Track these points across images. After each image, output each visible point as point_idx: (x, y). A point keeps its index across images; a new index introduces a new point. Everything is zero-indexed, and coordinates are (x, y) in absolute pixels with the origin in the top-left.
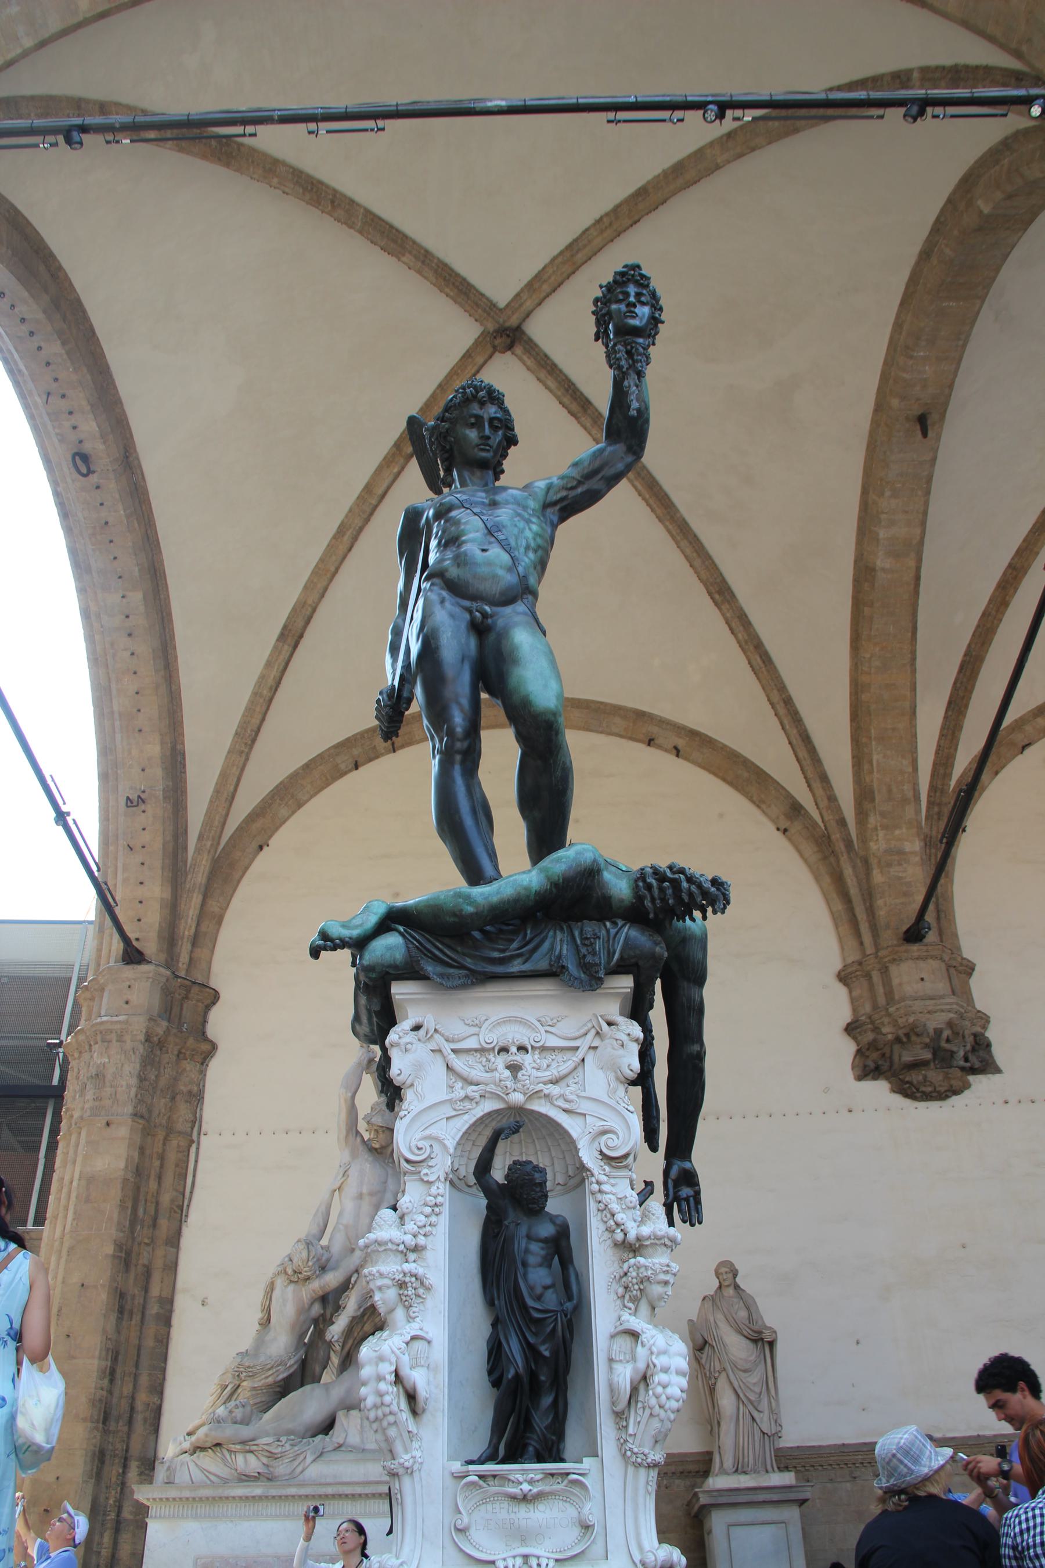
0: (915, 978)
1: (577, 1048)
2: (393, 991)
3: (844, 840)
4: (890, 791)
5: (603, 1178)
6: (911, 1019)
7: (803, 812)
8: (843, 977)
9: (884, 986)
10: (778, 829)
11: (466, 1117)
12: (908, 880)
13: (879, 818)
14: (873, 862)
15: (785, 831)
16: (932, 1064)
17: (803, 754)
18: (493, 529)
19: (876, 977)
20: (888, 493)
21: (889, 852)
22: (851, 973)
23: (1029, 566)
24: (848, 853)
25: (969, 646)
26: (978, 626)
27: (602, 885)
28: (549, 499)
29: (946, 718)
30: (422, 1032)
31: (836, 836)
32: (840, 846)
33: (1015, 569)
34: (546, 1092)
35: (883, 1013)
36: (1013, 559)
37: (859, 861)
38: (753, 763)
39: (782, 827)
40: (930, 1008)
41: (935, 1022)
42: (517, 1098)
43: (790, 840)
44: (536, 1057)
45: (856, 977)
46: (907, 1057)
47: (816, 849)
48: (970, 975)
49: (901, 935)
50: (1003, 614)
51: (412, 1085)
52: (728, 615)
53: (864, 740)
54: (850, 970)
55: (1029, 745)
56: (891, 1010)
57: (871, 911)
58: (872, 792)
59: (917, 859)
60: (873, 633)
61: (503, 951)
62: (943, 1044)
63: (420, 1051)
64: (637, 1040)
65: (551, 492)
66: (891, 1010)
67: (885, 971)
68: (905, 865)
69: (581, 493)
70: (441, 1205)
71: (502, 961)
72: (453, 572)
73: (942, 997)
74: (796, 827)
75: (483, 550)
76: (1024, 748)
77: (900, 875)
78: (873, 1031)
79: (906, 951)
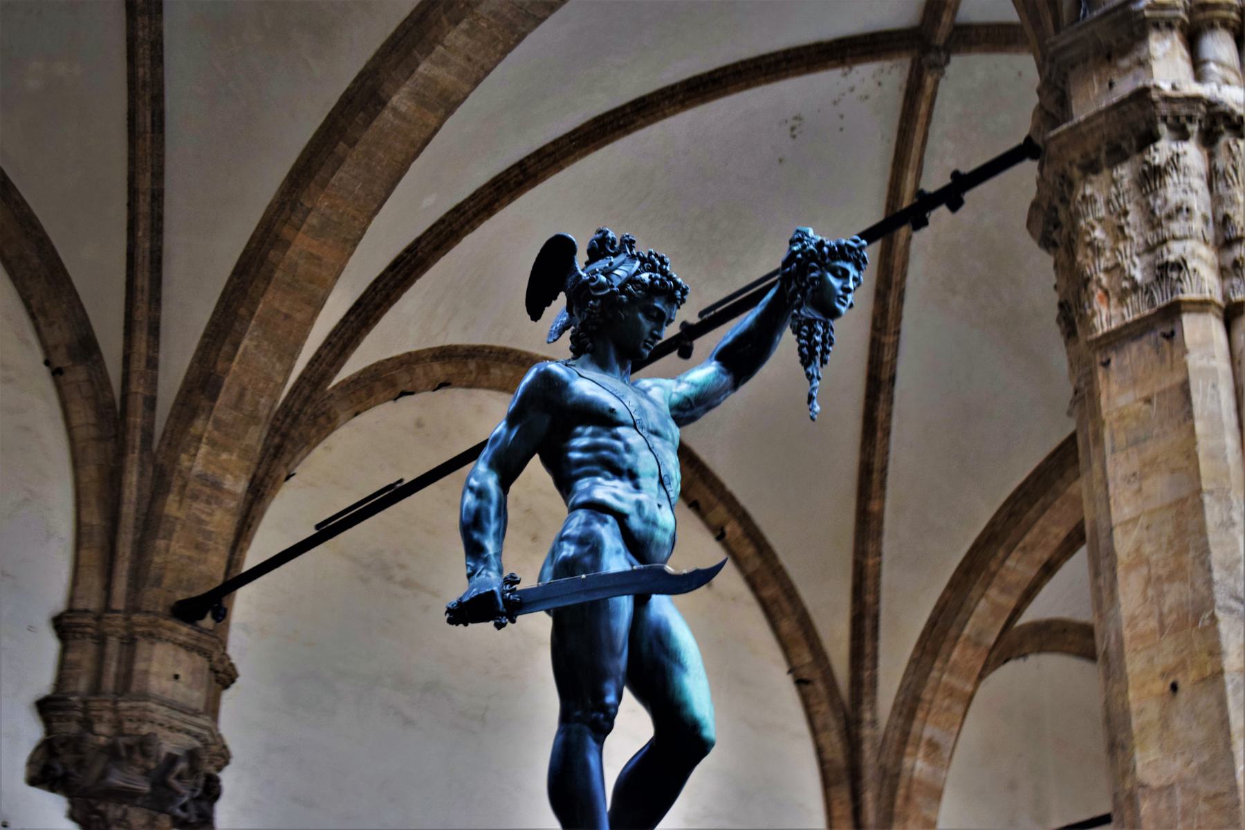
0: (166, 669)
3: (143, 429)
4: (241, 395)
6: (145, 729)
7: (95, 357)
8: (63, 626)
9: (119, 662)
10: (47, 363)
12: (210, 528)
13: (210, 426)
14: (176, 483)
15: (57, 373)
16: (139, 802)
17: (143, 281)
18: (666, 479)
19: (113, 646)
20: (464, 25)
21: (202, 477)
22: (79, 625)
23: (544, 178)
24: (141, 452)
25: (418, 241)
26: (441, 221)
29: (344, 321)
31: (136, 420)
32: (136, 438)
33: (524, 172)
35: (108, 704)
36: (528, 157)
37: (150, 469)
38: (53, 250)
39: (58, 365)
40: (176, 723)
41: (171, 743)
43: (59, 387)
45: (84, 634)
46: (117, 779)
47: (92, 420)
48: (226, 687)
49: (172, 603)
50: (481, 221)
52: (140, 33)
53: (242, 311)
54: (77, 620)
55: (412, 393)
56: (122, 705)
57: (142, 549)
58: (217, 386)
59: (233, 504)
60: (332, 181)
62: (172, 780)
66: (122, 705)
67: (130, 642)
68: (214, 506)
72: (635, 523)
73: (196, 713)
74: (79, 374)
75: (659, 506)
76: (403, 394)
77: (203, 516)
78: (79, 721)
79: (171, 630)
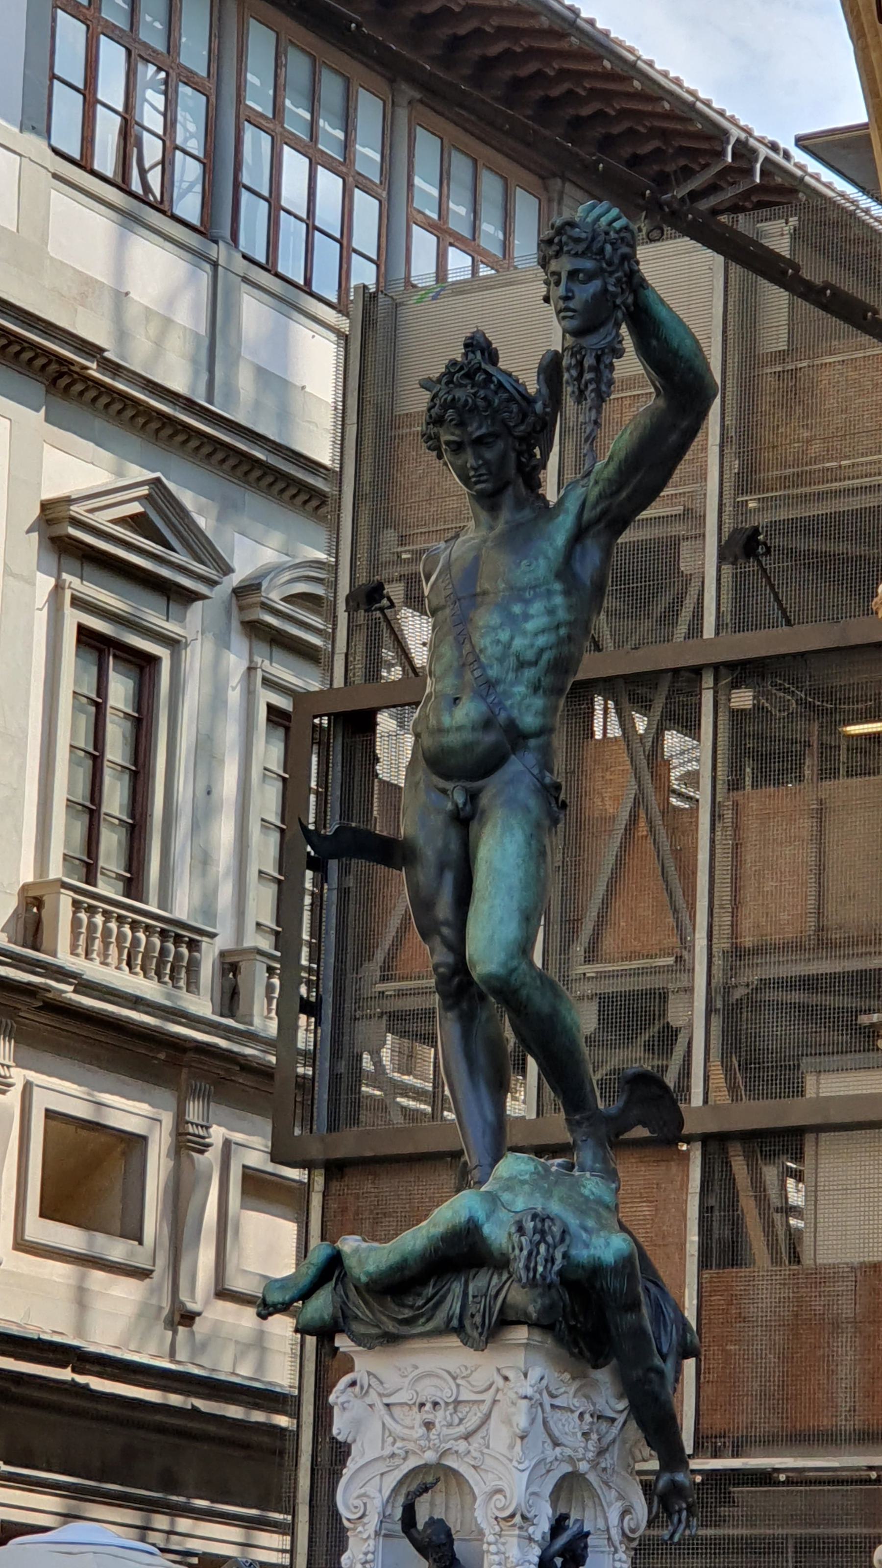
1: (483, 1401)
2: (337, 1344)
5: (491, 1538)
11: (396, 1472)
27: (483, 1239)
28: (586, 516)
30: (357, 1389)
34: (455, 1448)
42: (430, 1457)
44: (448, 1413)
51: (354, 1441)
61: (411, 1307)
63: (357, 1407)
64: (526, 1397)
65: (588, 505)
69: (629, 498)
70: (372, 1561)
71: (407, 1322)
